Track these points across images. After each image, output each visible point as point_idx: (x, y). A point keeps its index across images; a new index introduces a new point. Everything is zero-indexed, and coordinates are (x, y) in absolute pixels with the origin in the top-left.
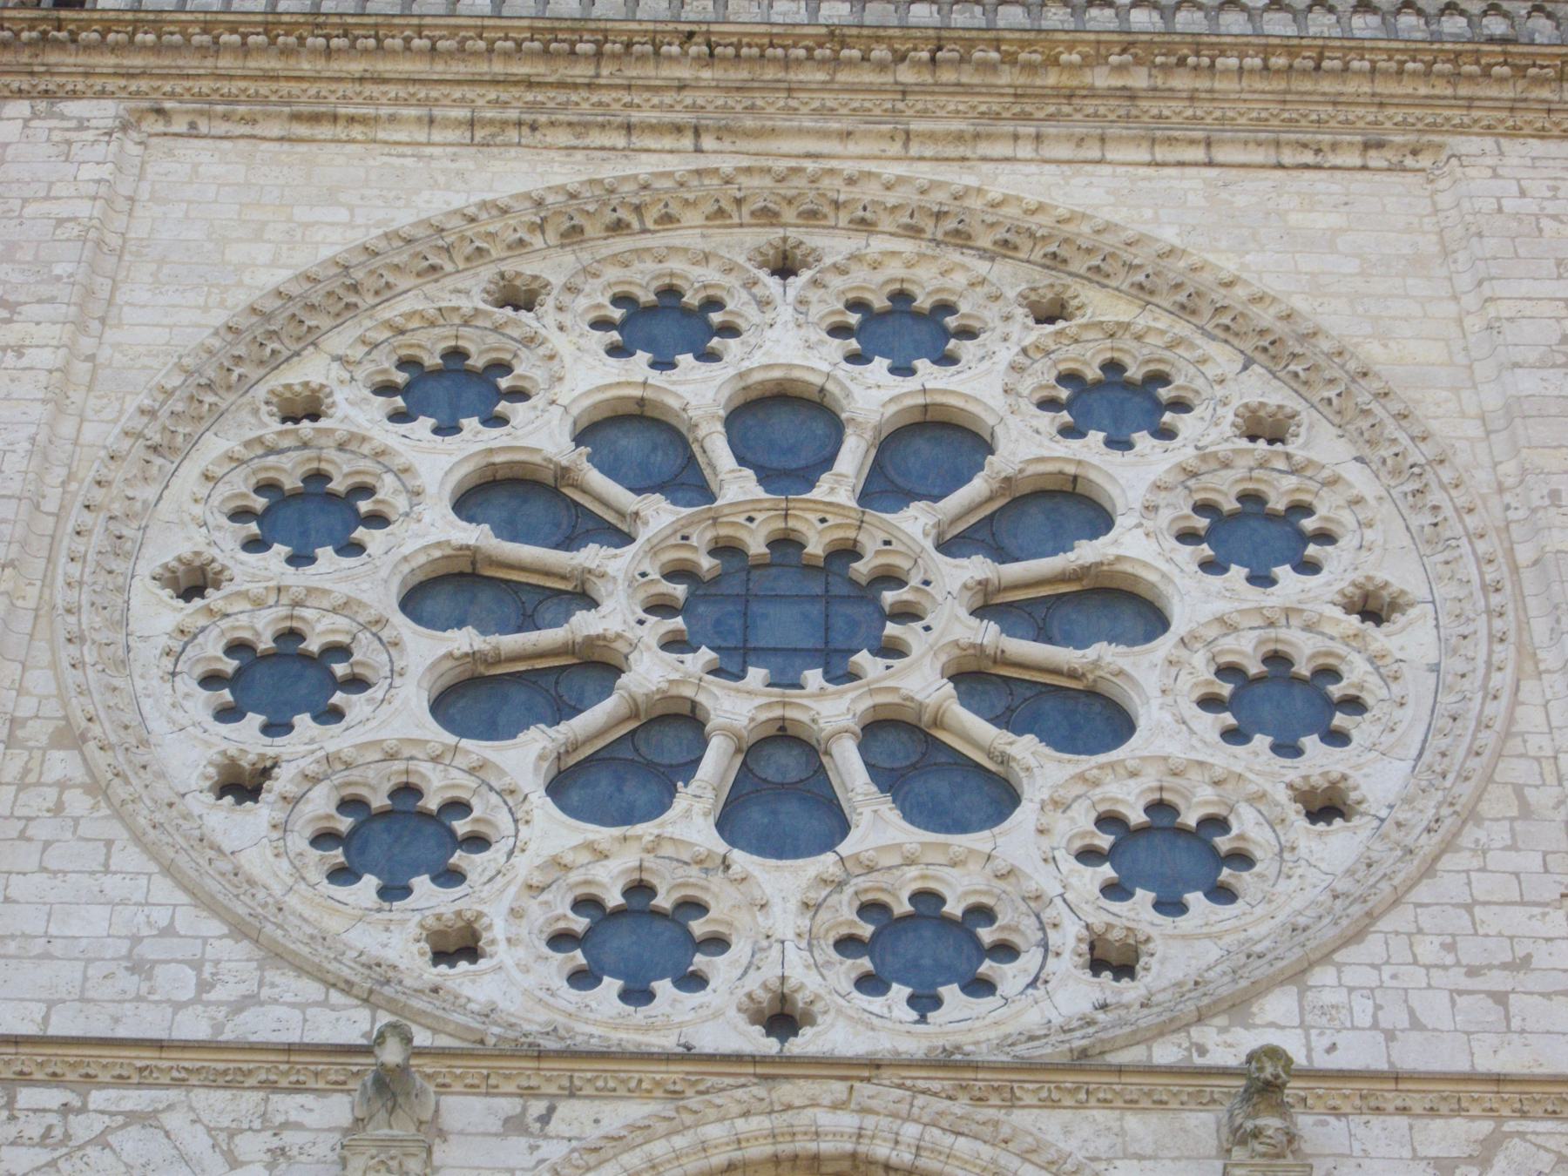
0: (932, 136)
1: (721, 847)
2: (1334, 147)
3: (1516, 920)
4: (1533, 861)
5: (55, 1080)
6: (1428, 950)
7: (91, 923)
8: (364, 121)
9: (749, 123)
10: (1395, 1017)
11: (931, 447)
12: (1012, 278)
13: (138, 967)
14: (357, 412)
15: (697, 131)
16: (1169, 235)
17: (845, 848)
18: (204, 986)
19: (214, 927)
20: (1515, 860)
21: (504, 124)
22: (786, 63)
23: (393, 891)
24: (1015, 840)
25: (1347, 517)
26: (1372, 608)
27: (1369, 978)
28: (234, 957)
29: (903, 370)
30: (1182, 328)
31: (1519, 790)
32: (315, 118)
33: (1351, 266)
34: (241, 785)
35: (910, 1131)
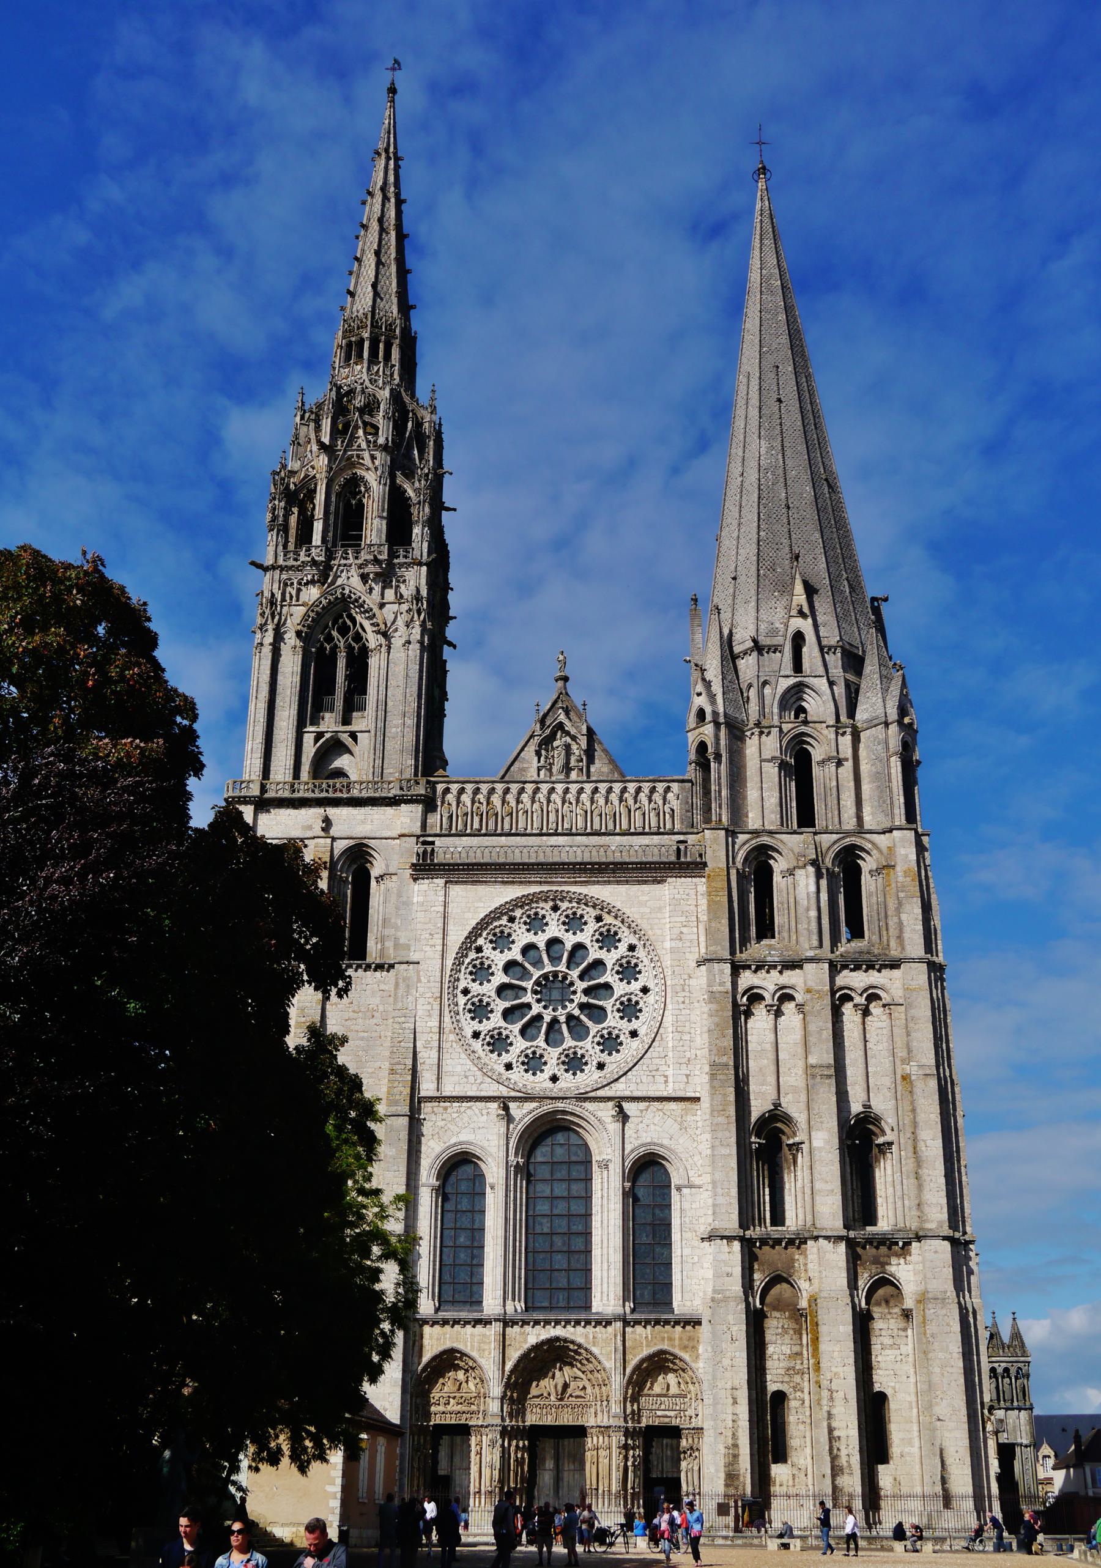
1: (546, 1046)
3: (657, 1061)
6: (645, 1068)
7: (459, 1069)
10: (638, 1081)
12: (594, 913)
13: (466, 1077)
14: (488, 950)
16: (618, 905)
17: (564, 1046)
21: (507, 882)
23: (499, 1055)
26: (645, 990)
28: (479, 1073)
30: (620, 925)
34: (476, 1035)
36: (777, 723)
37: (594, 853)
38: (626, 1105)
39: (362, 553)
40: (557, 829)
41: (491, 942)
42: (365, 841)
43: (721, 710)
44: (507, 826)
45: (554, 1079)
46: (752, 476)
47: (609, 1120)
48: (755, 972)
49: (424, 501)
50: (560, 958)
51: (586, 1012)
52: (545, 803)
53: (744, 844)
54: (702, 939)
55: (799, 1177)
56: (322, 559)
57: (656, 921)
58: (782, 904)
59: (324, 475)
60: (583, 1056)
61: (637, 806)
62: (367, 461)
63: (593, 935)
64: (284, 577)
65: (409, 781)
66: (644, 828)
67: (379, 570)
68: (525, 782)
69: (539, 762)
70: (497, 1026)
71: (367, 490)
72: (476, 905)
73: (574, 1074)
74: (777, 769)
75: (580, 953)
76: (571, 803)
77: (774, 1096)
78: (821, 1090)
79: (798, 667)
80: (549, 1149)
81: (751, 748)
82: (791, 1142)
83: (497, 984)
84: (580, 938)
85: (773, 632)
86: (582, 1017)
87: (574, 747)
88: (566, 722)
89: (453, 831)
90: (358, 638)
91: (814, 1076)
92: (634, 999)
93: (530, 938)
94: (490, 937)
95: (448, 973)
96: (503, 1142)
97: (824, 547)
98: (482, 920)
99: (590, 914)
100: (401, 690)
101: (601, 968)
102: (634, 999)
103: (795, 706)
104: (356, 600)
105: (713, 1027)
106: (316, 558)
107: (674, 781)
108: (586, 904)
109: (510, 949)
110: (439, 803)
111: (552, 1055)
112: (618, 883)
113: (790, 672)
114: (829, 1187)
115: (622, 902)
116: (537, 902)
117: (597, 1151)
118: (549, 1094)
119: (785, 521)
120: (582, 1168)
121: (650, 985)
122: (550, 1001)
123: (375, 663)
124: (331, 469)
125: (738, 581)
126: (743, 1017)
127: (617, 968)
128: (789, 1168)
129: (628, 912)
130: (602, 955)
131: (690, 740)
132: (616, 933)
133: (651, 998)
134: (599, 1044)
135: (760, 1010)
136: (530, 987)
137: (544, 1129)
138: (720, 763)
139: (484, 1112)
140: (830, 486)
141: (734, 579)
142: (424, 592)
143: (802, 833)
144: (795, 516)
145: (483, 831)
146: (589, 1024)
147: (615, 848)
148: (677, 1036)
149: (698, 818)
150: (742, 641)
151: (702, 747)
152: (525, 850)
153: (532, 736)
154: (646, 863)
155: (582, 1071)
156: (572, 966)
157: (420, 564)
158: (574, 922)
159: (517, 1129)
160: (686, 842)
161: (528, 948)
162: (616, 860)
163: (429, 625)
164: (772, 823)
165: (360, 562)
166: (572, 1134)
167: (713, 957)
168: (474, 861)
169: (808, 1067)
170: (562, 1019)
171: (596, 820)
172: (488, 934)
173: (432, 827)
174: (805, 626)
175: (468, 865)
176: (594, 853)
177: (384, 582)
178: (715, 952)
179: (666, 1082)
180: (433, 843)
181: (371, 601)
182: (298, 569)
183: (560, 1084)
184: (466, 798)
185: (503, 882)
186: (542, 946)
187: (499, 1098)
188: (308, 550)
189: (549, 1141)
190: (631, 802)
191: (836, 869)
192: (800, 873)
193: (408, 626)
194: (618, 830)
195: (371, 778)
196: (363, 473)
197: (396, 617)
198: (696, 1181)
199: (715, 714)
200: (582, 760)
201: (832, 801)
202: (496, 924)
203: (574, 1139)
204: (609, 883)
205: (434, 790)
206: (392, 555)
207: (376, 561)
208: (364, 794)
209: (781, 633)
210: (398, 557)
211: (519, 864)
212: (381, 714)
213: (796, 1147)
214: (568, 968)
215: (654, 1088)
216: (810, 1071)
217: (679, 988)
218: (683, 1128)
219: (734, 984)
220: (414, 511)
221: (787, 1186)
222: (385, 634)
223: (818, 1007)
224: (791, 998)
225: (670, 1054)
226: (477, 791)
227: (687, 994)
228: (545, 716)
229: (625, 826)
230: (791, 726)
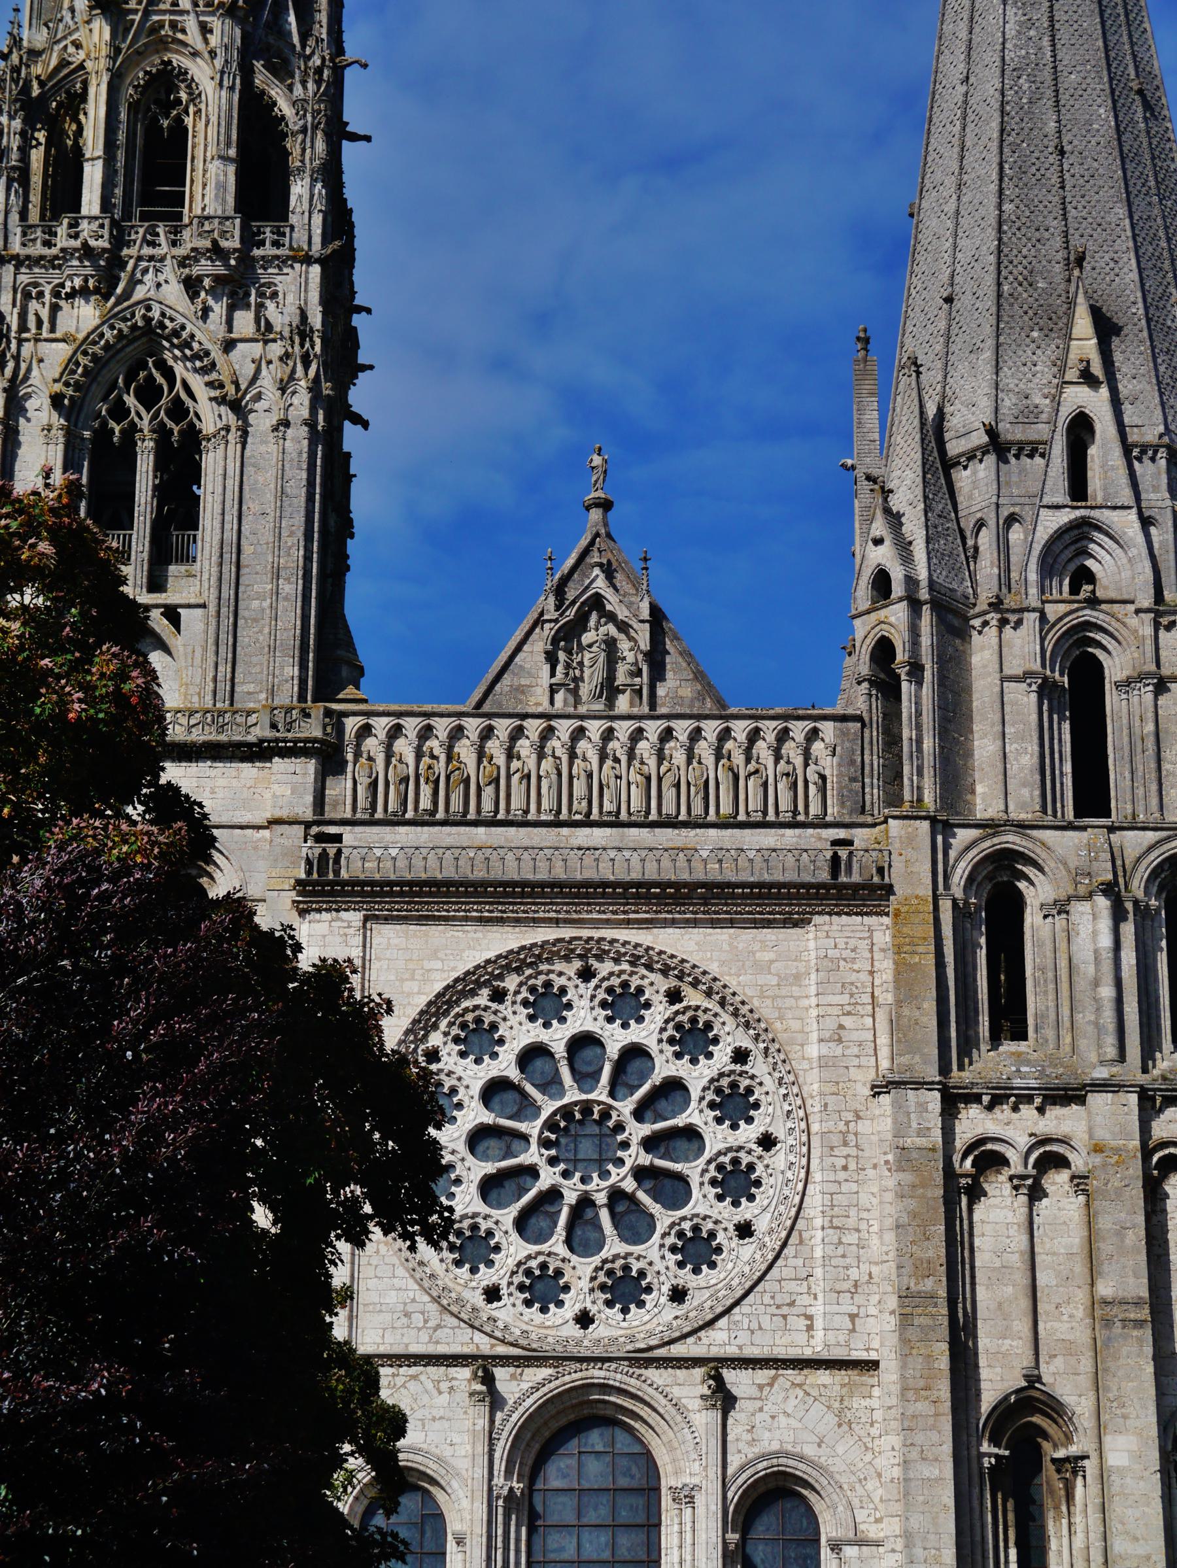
3: (792, 1286)
4: (800, 1262)
6: (767, 1299)
13: (407, 1315)
16: (714, 969)
17: (604, 1254)
18: (426, 1321)
19: (427, 1298)
23: (474, 1270)
26: (767, 1142)
28: (433, 1308)
29: (625, 1026)
30: (717, 1009)
32: (427, 918)
33: (774, 981)
35: (619, 1376)
36: (1033, 600)
37: (666, 863)
38: (730, 1376)
39: (186, 234)
40: (589, 813)
41: (457, 1040)
43: (922, 574)
44: (487, 806)
45: (584, 1319)
46: (988, 85)
47: (697, 1404)
48: (990, 1108)
49: (315, 127)
50: (596, 1075)
51: (648, 1184)
52: (565, 759)
53: (968, 848)
54: (883, 1040)
55: (1079, 1528)
56: (103, 243)
57: (790, 1002)
58: (1043, 970)
59: (103, 63)
60: (642, 1274)
61: (752, 767)
62: (193, 36)
63: (663, 1030)
64: (23, 279)
65: (289, 710)
66: (765, 813)
67: (223, 271)
68: (525, 716)
69: (553, 675)
70: (470, 1210)
71: (194, 97)
72: (428, 965)
73: (625, 1311)
74: (1034, 697)
75: (636, 1064)
76: (617, 760)
77: (1027, 1360)
78: (1124, 1351)
79: (1078, 488)
80: (573, 1462)
81: (982, 651)
82: (1061, 1454)
83: (469, 1126)
84: (636, 1034)
85: (1029, 415)
86: (641, 1196)
87: (624, 645)
88: (608, 593)
89: (379, 814)
90: (178, 411)
91: (1108, 1323)
92: (745, 1159)
93: (533, 1033)
94: (455, 1031)
96: (482, 1448)
97: (1134, 236)
98: (439, 995)
99: (656, 986)
100: (268, 523)
101: (678, 1096)
102: (745, 1159)
103: (1072, 567)
104: (176, 333)
105: (905, 1219)
106: (92, 243)
107: (825, 718)
108: (649, 967)
109: (494, 1056)
110: (350, 757)
111: (581, 1272)
112: (714, 924)
113: (1062, 498)
114: (1141, 1549)
115: (722, 963)
116: (549, 961)
117: (669, 1468)
118: (575, 1351)
119: (1055, 179)
120: (640, 1501)
121: (779, 1131)
122: (576, 1161)
123: (214, 463)
124: (118, 51)
125: (957, 305)
126: (964, 1199)
127: (710, 1096)
128: (1057, 1507)
129: (733, 983)
130: (681, 1069)
131: (859, 635)
132: (709, 1026)
133: (779, 1158)
134: (673, 1249)
135: (998, 1187)
136: (535, 1133)
137: (563, 1421)
138: (920, 683)
139: (444, 1386)
140: (1147, 106)
141: (949, 300)
142: (316, 320)
143: (1084, 828)
144: (1076, 170)
145: (440, 815)
146: (655, 1208)
147: (708, 852)
148: (833, 1236)
149: (874, 794)
150: (966, 426)
151: (883, 650)
152: (526, 856)
153: (539, 622)
154: (771, 885)
155: (641, 1304)
156: (621, 1091)
157: (308, 260)
158: (624, 1004)
159: (510, 1421)
160: (850, 843)
161: (532, 1055)
162: (711, 877)
163: (327, 388)
164: (1023, 806)
165: (181, 251)
166: (621, 1435)
167: (906, 1077)
168: (423, 876)
169: (1095, 1303)
170: (601, 1198)
171: (669, 794)
172: (451, 1024)
173: (335, 805)
174: (1096, 402)
175: (411, 884)
176: (666, 863)
177: (232, 295)
178: (909, 1068)
179: (810, 1328)
180: (338, 838)
181: (209, 334)
182: (51, 263)
183: (598, 1330)
184: (405, 747)
186: (559, 1049)
187: (475, 1357)
188: (74, 225)
189: (573, 1446)
190: (738, 759)
191: (1153, 902)
192: (1080, 909)
193: (283, 390)
194: (712, 817)
195: (209, 705)
196: (186, 63)
197: (258, 371)
198: (872, 1531)
199: (911, 582)
200: (639, 673)
201: (1144, 762)
202: (466, 1004)
203: (622, 1441)
204: (695, 923)
205: (340, 729)
206: (250, 239)
207: (217, 251)
208: (198, 736)
209: (1044, 417)
210: (262, 243)
211: (514, 884)
212: (229, 570)
213: (1072, 1466)
214: (612, 1094)
215: (784, 1341)
216: (1101, 1311)
217: (836, 1140)
218: (845, 1423)
219: (948, 1133)
220: (293, 146)
221: (1053, 1545)
222: (236, 406)
223: (1116, 1182)
224: (1061, 1162)
225: (818, 1272)
226: (426, 733)
227: (853, 1152)
228: (565, 580)
229: (726, 808)
230: (1062, 608)
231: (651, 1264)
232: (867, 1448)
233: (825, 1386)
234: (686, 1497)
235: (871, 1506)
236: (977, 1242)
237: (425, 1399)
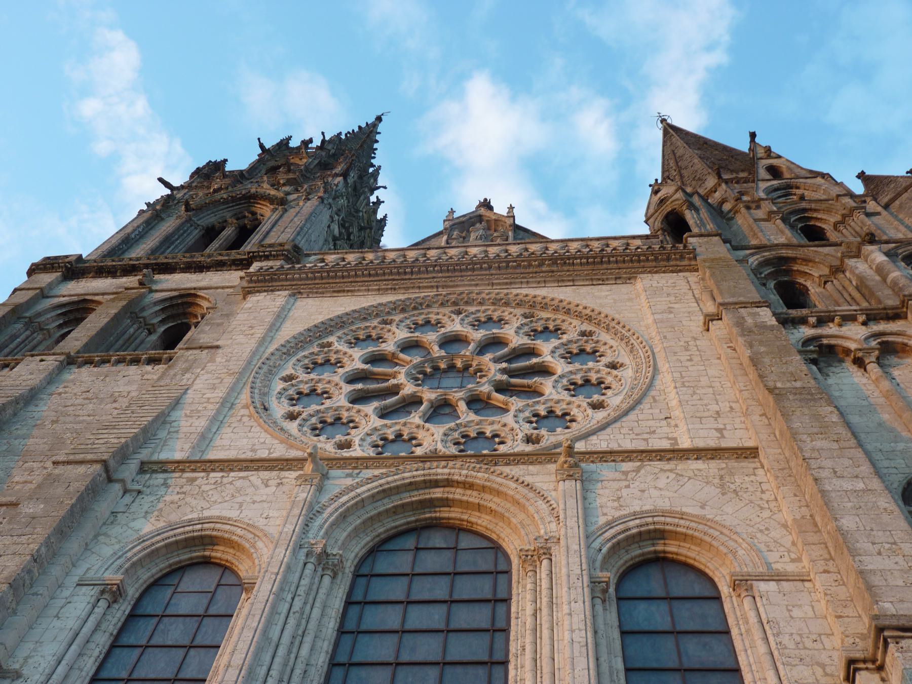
0: (499, 284)
2: (607, 279)
3: (651, 423)
5: (222, 470)
8: (351, 291)
9: (451, 284)
11: (495, 342)
15: (437, 287)
20: (651, 411)
21: (387, 289)
22: (461, 271)
24: (509, 418)
25: (609, 351)
27: (608, 437)
31: (653, 397)
32: (339, 292)
34: (292, 417)
35: (464, 472)
42: (192, 292)
68: (429, 249)
95: (266, 355)
116: (428, 306)
133: (627, 374)
139: (273, 483)
157: (337, 175)
161: (408, 346)
185: (380, 291)
225: (677, 413)
231: (505, 425)
232: (762, 508)
233: (700, 470)
234: (542, 552)
235: (782, 549)
236: (837, 394)
237: (250, 490)
